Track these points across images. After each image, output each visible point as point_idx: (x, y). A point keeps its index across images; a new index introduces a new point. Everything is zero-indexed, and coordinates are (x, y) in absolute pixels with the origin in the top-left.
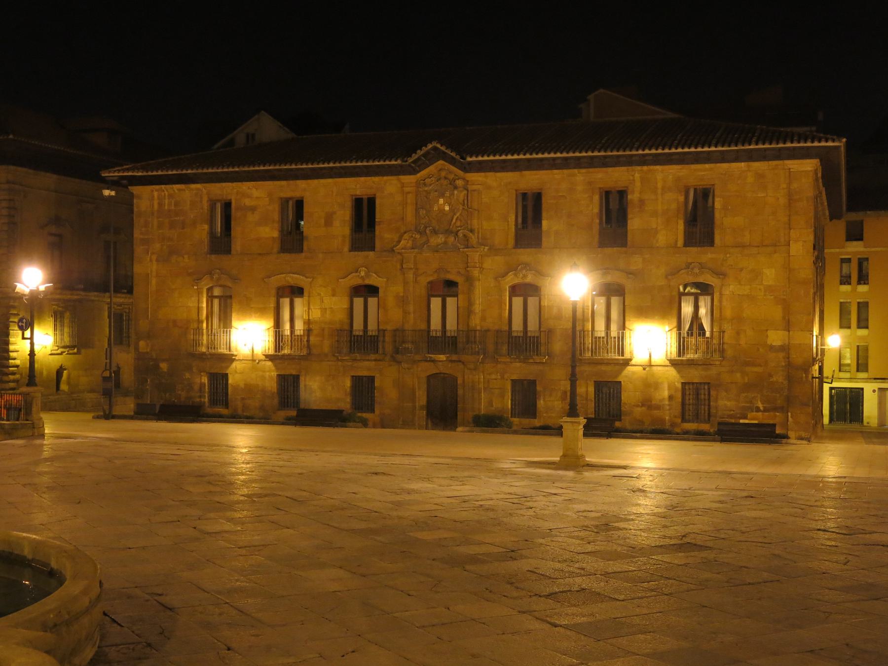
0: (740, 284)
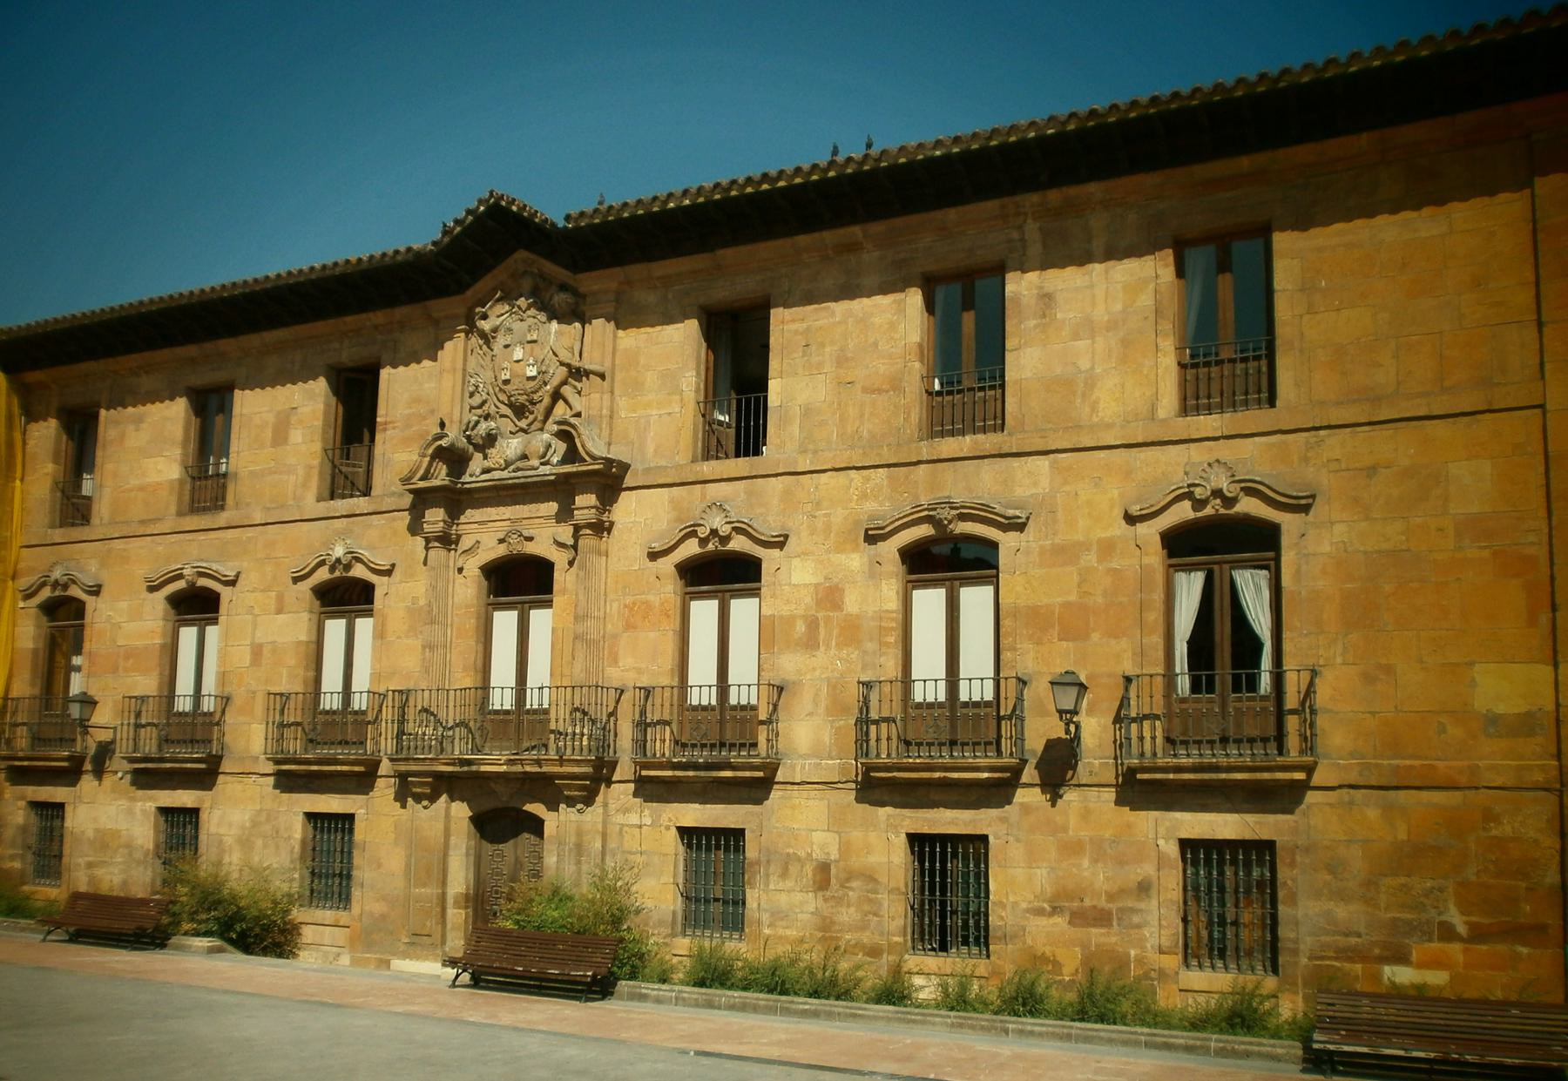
0: (1367, 518)
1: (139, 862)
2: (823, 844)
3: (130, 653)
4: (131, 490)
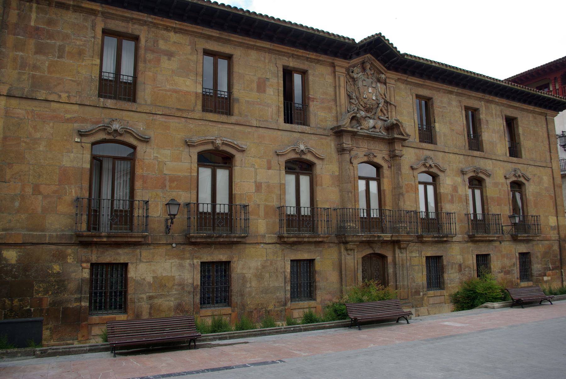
1: (189, 293)
2: (459, 258)
3: (173, 179)
4: (166, 90)
